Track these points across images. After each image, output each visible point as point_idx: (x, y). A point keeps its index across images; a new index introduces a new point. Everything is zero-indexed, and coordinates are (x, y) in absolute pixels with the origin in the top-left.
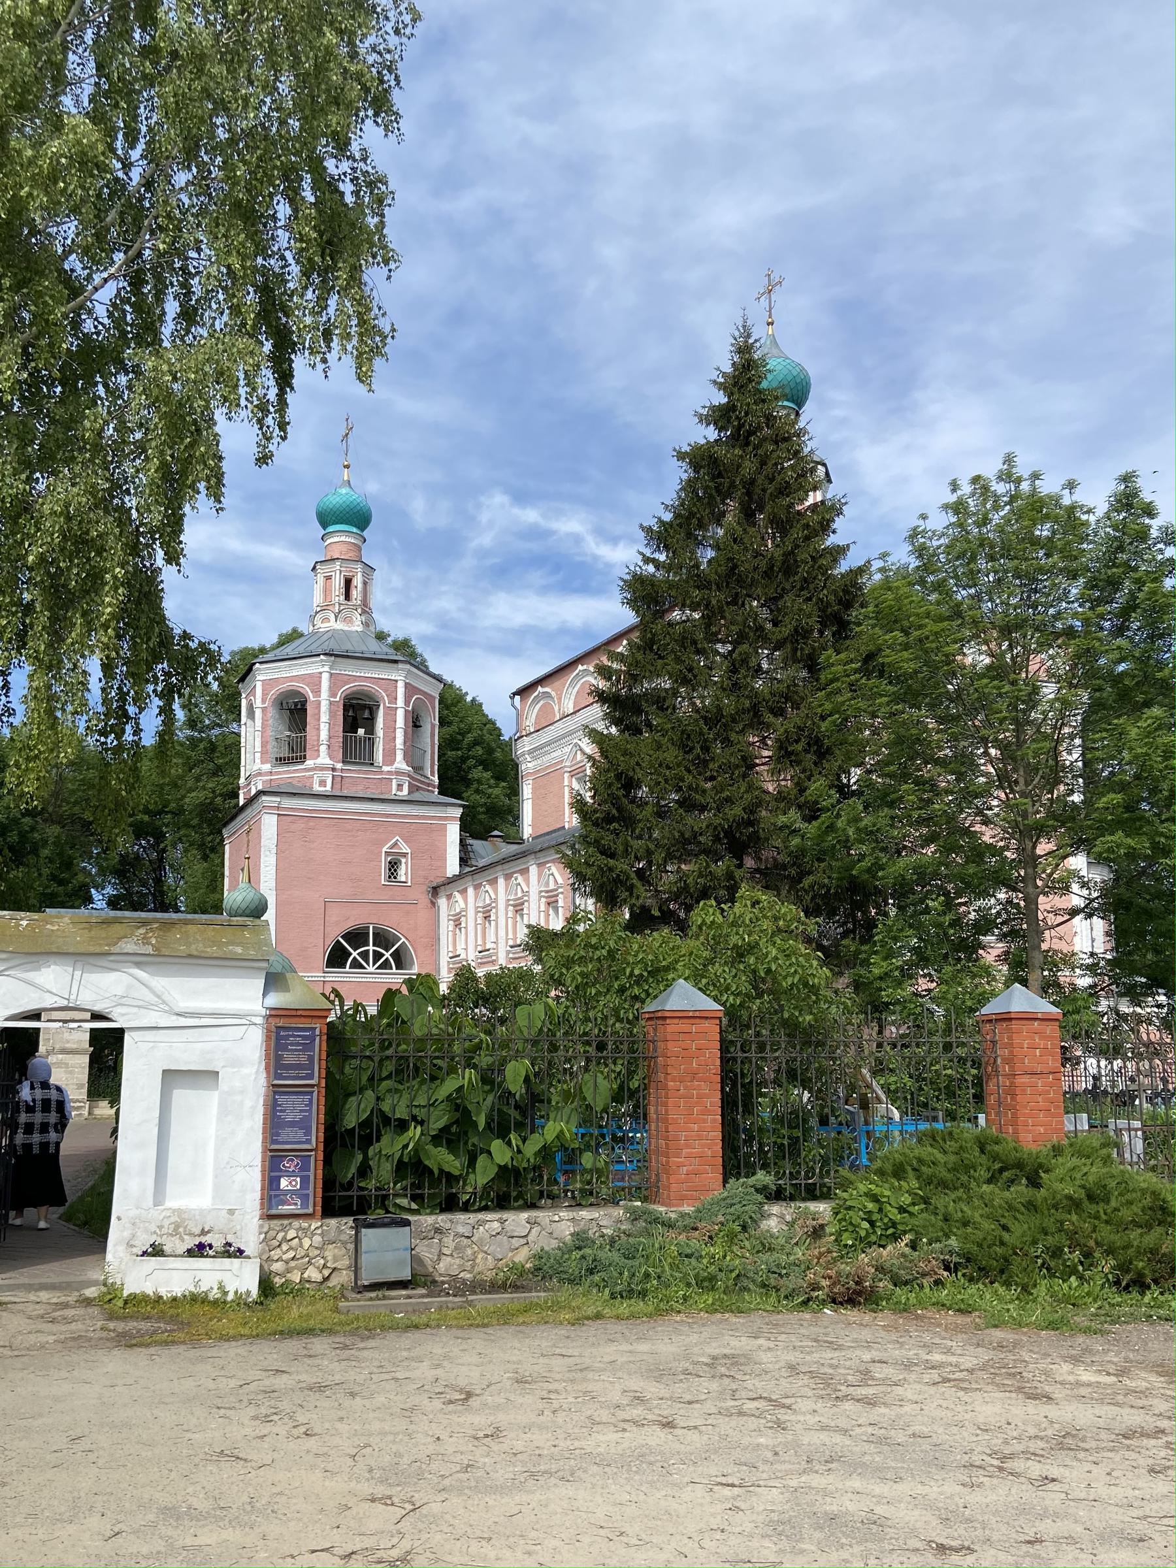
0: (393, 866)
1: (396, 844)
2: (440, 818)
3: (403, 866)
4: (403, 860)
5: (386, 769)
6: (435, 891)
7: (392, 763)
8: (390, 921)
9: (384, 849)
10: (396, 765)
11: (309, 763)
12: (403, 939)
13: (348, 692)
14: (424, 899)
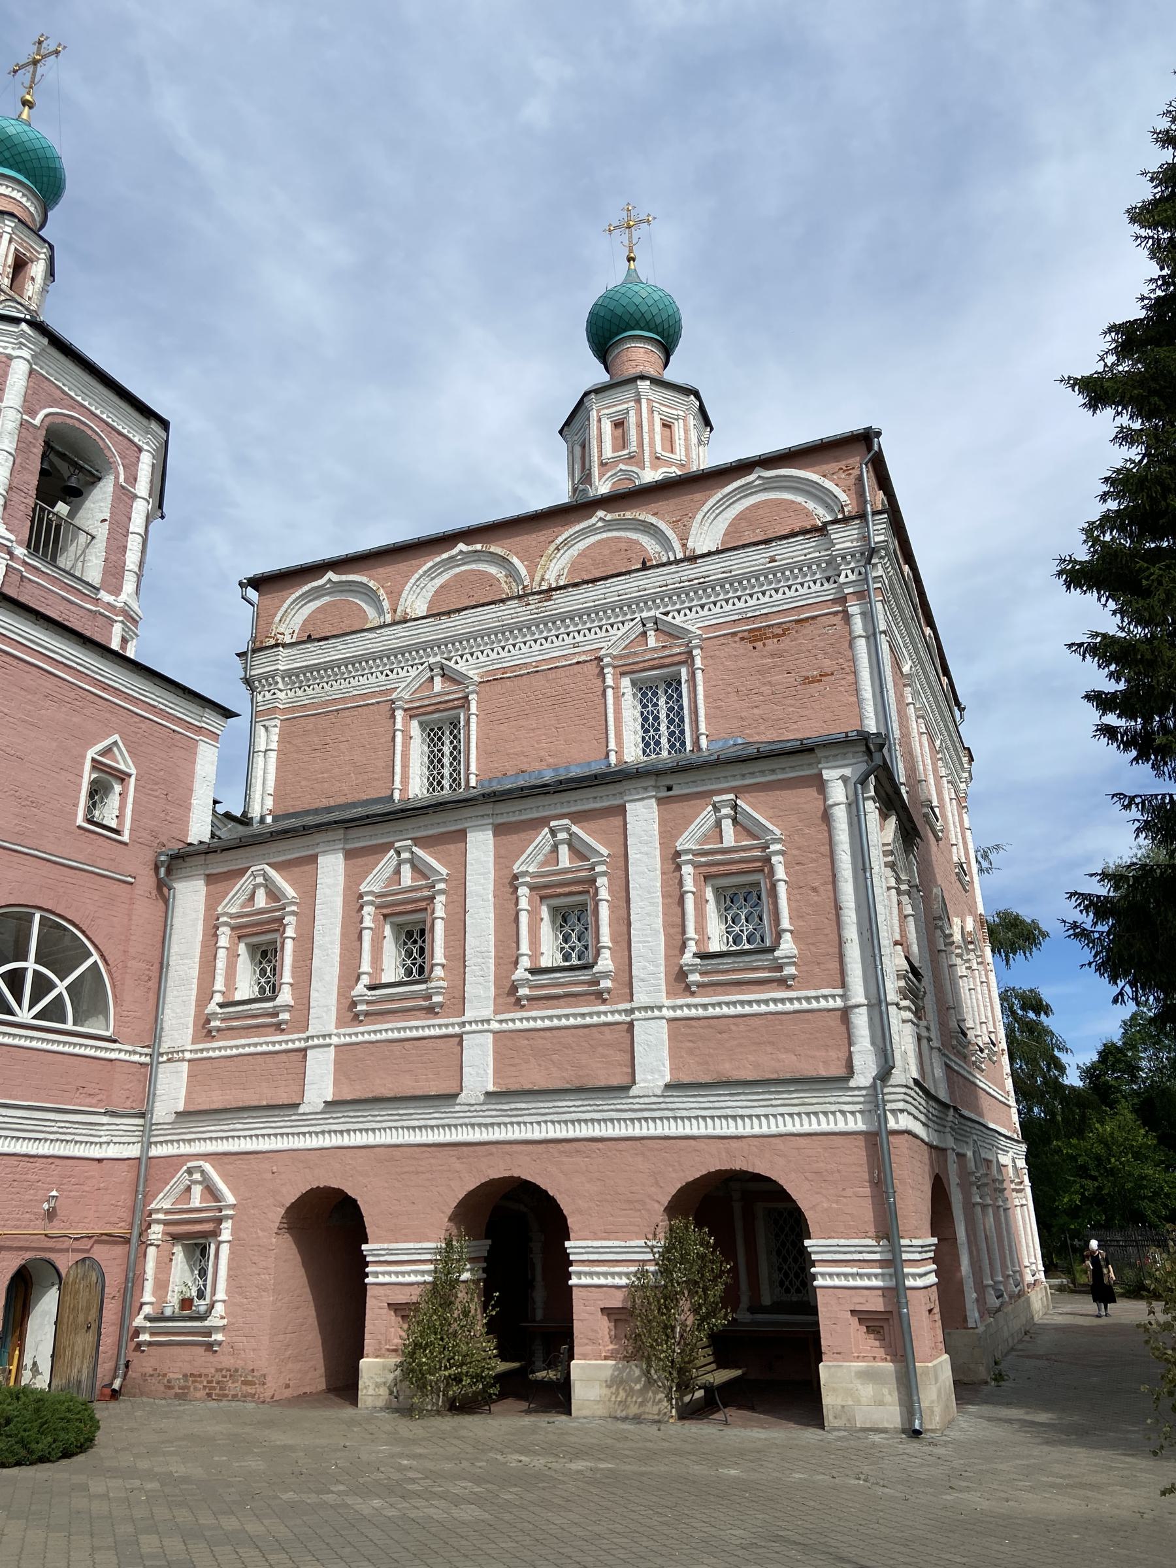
0: (98, 791)
1: (107, 751)
2: (189, 726)
3: (113, 801)
4: (118, 788)
5: (105, 596)
6: (177, 861)
7: (117, 591)
8: (80, 906)
9: (91, 753)
10: (123, 597)
12: (95, 957)
13: (58, 420)
14: (146, 881)
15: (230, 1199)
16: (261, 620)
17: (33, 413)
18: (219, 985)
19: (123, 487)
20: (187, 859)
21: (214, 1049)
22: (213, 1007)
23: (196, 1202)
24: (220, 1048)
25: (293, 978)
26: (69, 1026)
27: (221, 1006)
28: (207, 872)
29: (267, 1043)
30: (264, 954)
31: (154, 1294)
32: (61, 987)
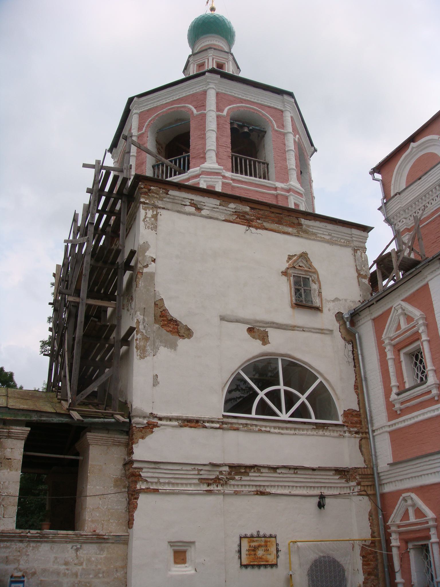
11: (193, 171)
15: (430, 514)
16: (385, 186)
17: (222, 111)
18: (394, 382)
19: (277, 131)
20: (361, 313)
21: (401, 422)
22: (393, 396)
23: (412, 519)
24: (404, 421)
25: (434, 366)
26: (313, 420)
27: (398, 394)
28: (373, 317)
29: (430, 411)
30: (417, 357)
31: (403, 577)
32: (303, 398)
